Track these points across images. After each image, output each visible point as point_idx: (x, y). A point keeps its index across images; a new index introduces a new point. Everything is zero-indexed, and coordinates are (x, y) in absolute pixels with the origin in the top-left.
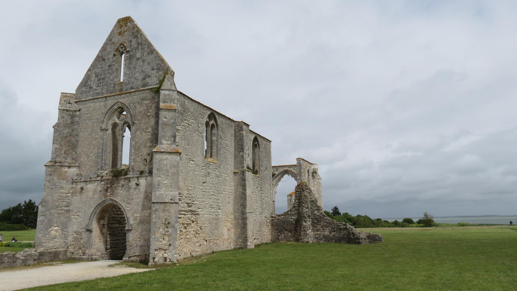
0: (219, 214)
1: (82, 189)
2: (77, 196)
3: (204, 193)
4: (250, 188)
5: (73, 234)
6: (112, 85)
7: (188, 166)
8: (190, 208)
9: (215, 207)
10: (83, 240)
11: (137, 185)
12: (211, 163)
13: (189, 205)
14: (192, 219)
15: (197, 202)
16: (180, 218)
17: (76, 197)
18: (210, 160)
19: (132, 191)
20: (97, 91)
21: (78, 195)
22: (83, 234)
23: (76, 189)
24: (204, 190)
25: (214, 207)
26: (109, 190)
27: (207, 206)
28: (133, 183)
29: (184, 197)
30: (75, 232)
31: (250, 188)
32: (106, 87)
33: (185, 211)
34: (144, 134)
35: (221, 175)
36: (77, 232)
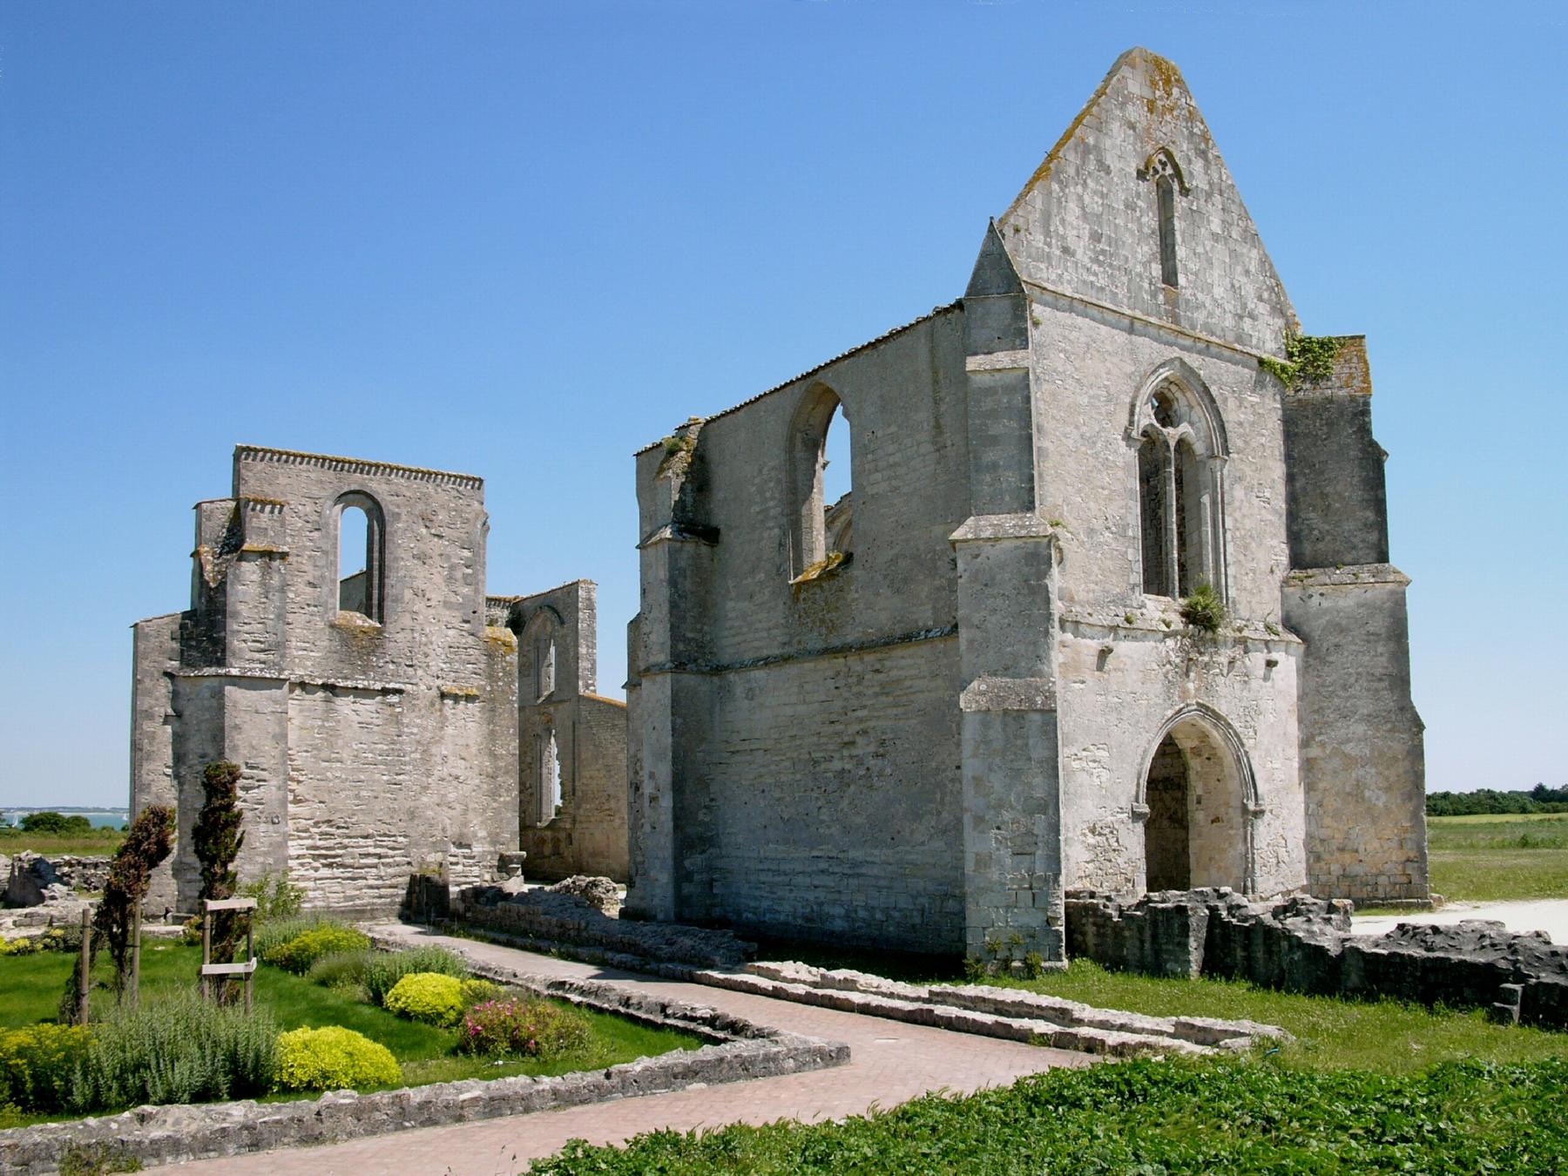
1: (1104, 653)
2: (1083, 682)
5: (1085, 835)
6: (1146, 286)
10: (1125, 855)
11: (1271, 664)
17: (1082, 686)
19: (1254, 684)
20: (1092, 278)
21: (1087, 677)
22: (1123, 832)
23: (1078, 653)
26: (1192, 675)
28: (1258, 659)
30: (1093, 831)
32: (1125, 279)
34: (1256, 501)
36: (1100, 824)
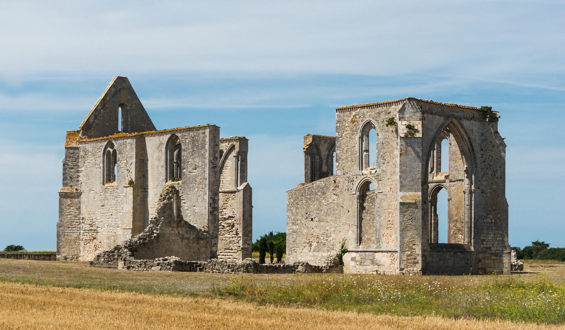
0: (118, 231)
3: (103, 214)
4: (128, 204)
7: (89, 195)
8: (92, 228)
9: (113, 225)
12: (108, 188)
13: (91, 225)
14: (94, 236)
15: (97, 223)
16: (85, 235)
18: (107, 185)
24: (102, 212)
25: (112, 225)
27: (106, 225)
29: (86, 220)
31: (128, 204)
33: (87, 230)
35: (119, 196)
